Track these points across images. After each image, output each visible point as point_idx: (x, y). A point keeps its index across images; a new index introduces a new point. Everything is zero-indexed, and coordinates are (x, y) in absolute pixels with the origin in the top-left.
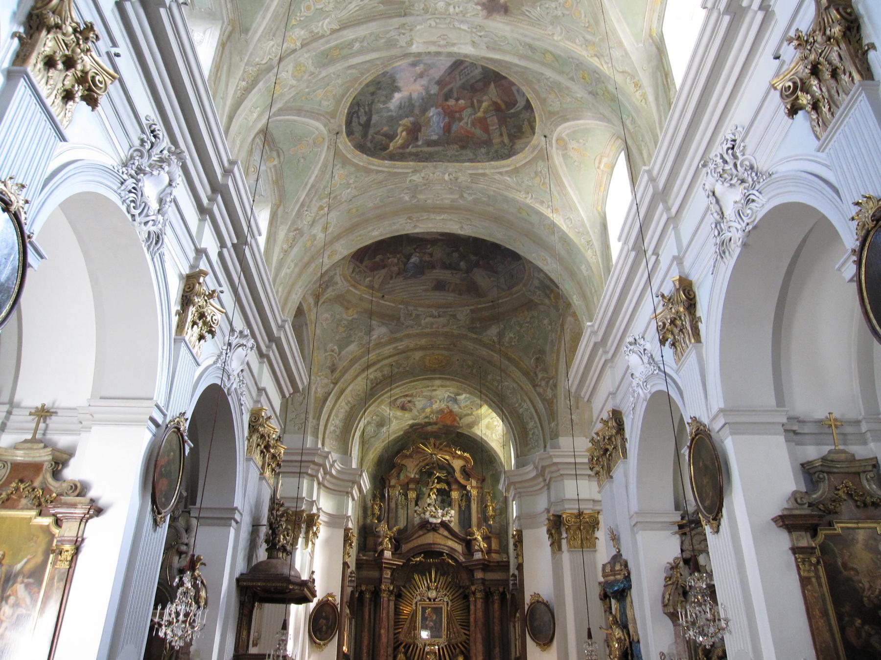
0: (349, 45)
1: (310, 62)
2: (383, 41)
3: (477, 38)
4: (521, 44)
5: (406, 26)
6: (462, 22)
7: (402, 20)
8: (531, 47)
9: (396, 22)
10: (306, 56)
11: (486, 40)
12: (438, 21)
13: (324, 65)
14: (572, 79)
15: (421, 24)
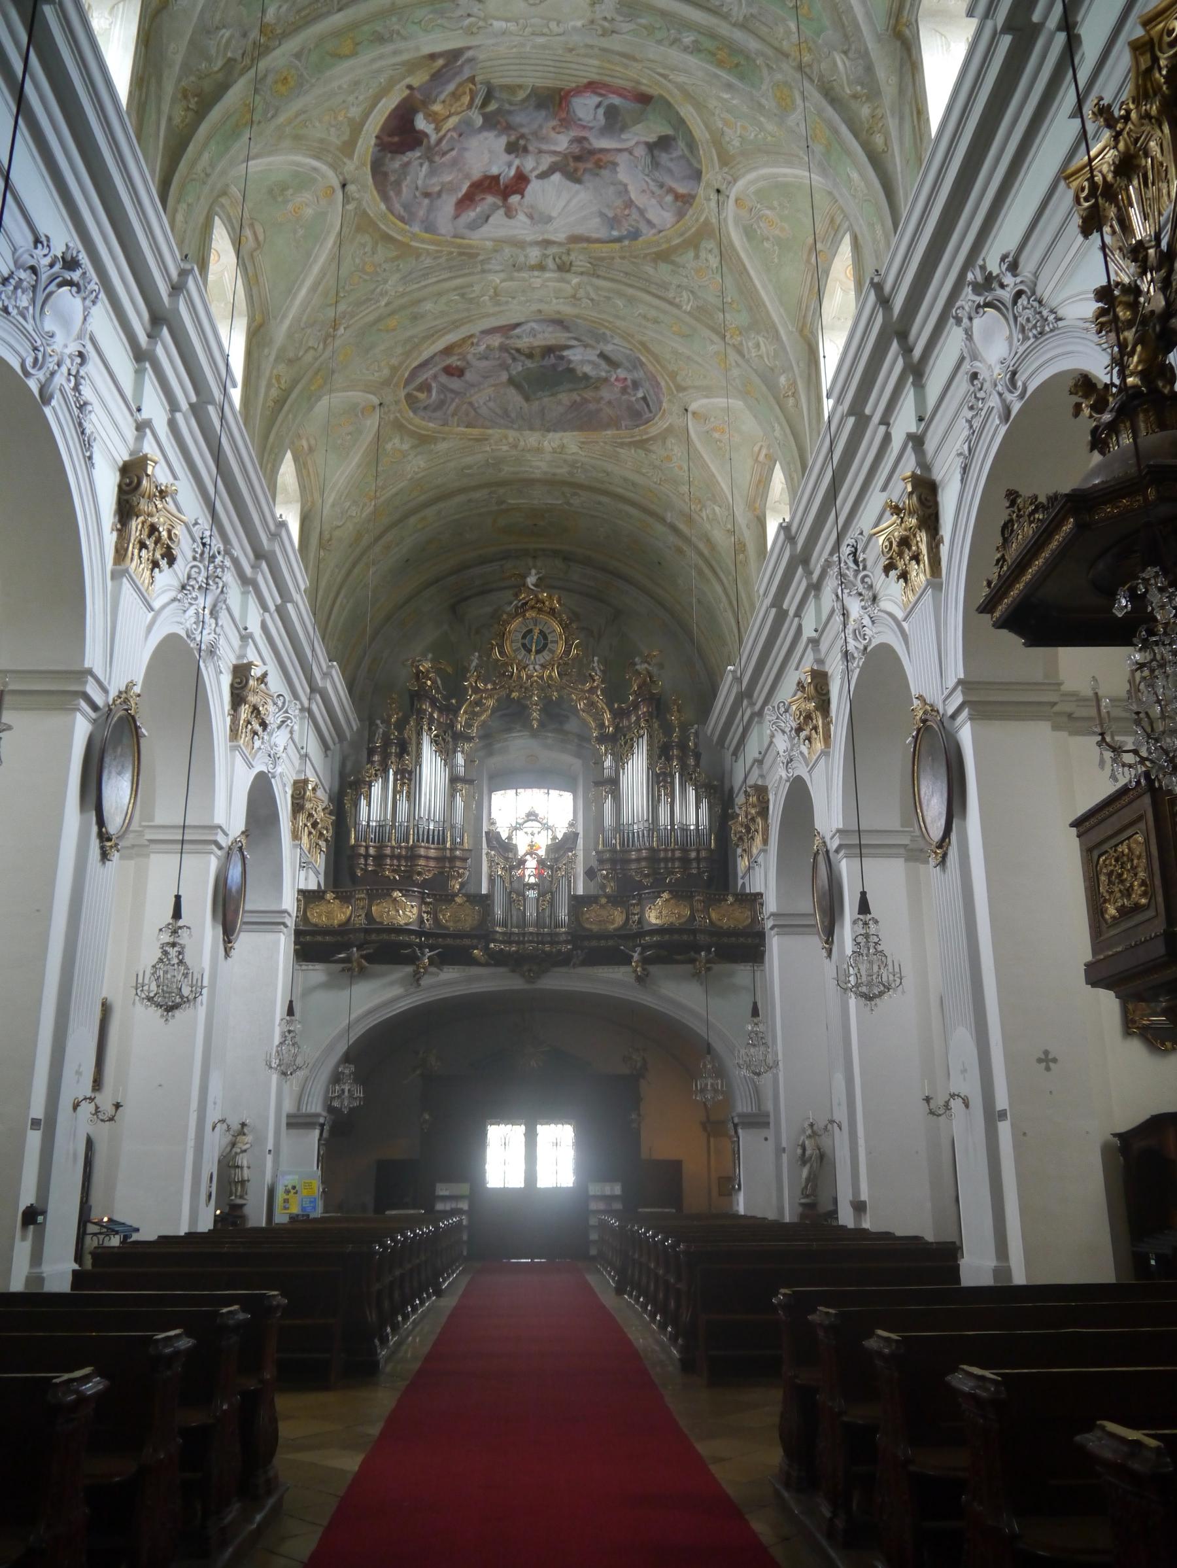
0: (699, 51)
1: (764, 87)
2: (643, 21)
3: (475, 10)
4: (398, 33)
5: (600, 32)
6: (504, 33)
7: (605, 43)
8: (380, 39)
9: (614, 43)
10: (763, 101)
11: (460, 12)
12: (545, 30)
13: (747, 57)
14: (298, 56)
15: (575, 29)
